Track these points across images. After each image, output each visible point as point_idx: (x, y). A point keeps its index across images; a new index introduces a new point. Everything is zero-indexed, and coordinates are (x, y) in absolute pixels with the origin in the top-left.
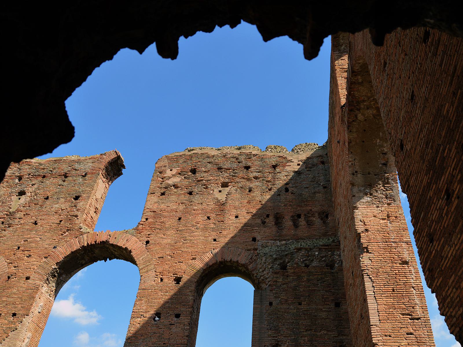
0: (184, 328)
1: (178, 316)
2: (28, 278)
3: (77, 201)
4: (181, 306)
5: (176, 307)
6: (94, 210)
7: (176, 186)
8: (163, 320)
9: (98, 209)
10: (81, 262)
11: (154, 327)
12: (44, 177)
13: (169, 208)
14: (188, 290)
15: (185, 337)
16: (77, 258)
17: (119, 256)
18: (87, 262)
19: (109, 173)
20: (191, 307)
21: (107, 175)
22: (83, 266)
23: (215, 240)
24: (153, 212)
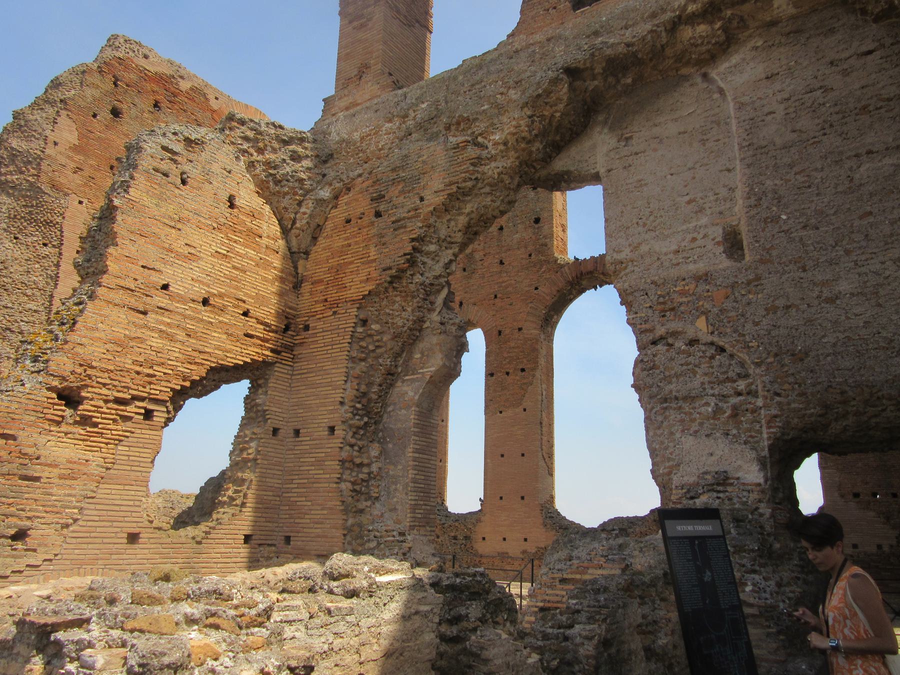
2: (520, 329)
22: (571, 300)
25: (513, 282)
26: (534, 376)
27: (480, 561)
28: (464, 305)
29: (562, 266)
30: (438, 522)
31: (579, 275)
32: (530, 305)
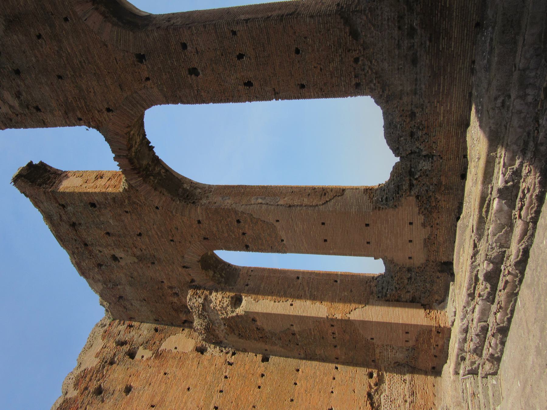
0: (196, 33)
1: (184, 46)
2: (199, 222)
3: (96, 204)
4: (170, 45)
5: (173, 51)
6: (99, 180)
7: (18, 95)
9: (97, 176)
10: (163, 174)
11: (207, 72)
12: (86, 245)
13: (52, 96)
14: (147, 40)
15: (207, 29)
16: (160, 180)
17: (141, 135)
18: (161, 167)
19: (47, 179)
20: (168, 30)
21: (50, 180)
22: (168, 170)
23: (66, 19)
24: (67, 114)
25: (155, 226)
26: (243, 213)
27: (433, 262)
28: (185, 265)
29: (130, 186)
30: (394, 292)
31: (136, 172)
32: (174, 213)
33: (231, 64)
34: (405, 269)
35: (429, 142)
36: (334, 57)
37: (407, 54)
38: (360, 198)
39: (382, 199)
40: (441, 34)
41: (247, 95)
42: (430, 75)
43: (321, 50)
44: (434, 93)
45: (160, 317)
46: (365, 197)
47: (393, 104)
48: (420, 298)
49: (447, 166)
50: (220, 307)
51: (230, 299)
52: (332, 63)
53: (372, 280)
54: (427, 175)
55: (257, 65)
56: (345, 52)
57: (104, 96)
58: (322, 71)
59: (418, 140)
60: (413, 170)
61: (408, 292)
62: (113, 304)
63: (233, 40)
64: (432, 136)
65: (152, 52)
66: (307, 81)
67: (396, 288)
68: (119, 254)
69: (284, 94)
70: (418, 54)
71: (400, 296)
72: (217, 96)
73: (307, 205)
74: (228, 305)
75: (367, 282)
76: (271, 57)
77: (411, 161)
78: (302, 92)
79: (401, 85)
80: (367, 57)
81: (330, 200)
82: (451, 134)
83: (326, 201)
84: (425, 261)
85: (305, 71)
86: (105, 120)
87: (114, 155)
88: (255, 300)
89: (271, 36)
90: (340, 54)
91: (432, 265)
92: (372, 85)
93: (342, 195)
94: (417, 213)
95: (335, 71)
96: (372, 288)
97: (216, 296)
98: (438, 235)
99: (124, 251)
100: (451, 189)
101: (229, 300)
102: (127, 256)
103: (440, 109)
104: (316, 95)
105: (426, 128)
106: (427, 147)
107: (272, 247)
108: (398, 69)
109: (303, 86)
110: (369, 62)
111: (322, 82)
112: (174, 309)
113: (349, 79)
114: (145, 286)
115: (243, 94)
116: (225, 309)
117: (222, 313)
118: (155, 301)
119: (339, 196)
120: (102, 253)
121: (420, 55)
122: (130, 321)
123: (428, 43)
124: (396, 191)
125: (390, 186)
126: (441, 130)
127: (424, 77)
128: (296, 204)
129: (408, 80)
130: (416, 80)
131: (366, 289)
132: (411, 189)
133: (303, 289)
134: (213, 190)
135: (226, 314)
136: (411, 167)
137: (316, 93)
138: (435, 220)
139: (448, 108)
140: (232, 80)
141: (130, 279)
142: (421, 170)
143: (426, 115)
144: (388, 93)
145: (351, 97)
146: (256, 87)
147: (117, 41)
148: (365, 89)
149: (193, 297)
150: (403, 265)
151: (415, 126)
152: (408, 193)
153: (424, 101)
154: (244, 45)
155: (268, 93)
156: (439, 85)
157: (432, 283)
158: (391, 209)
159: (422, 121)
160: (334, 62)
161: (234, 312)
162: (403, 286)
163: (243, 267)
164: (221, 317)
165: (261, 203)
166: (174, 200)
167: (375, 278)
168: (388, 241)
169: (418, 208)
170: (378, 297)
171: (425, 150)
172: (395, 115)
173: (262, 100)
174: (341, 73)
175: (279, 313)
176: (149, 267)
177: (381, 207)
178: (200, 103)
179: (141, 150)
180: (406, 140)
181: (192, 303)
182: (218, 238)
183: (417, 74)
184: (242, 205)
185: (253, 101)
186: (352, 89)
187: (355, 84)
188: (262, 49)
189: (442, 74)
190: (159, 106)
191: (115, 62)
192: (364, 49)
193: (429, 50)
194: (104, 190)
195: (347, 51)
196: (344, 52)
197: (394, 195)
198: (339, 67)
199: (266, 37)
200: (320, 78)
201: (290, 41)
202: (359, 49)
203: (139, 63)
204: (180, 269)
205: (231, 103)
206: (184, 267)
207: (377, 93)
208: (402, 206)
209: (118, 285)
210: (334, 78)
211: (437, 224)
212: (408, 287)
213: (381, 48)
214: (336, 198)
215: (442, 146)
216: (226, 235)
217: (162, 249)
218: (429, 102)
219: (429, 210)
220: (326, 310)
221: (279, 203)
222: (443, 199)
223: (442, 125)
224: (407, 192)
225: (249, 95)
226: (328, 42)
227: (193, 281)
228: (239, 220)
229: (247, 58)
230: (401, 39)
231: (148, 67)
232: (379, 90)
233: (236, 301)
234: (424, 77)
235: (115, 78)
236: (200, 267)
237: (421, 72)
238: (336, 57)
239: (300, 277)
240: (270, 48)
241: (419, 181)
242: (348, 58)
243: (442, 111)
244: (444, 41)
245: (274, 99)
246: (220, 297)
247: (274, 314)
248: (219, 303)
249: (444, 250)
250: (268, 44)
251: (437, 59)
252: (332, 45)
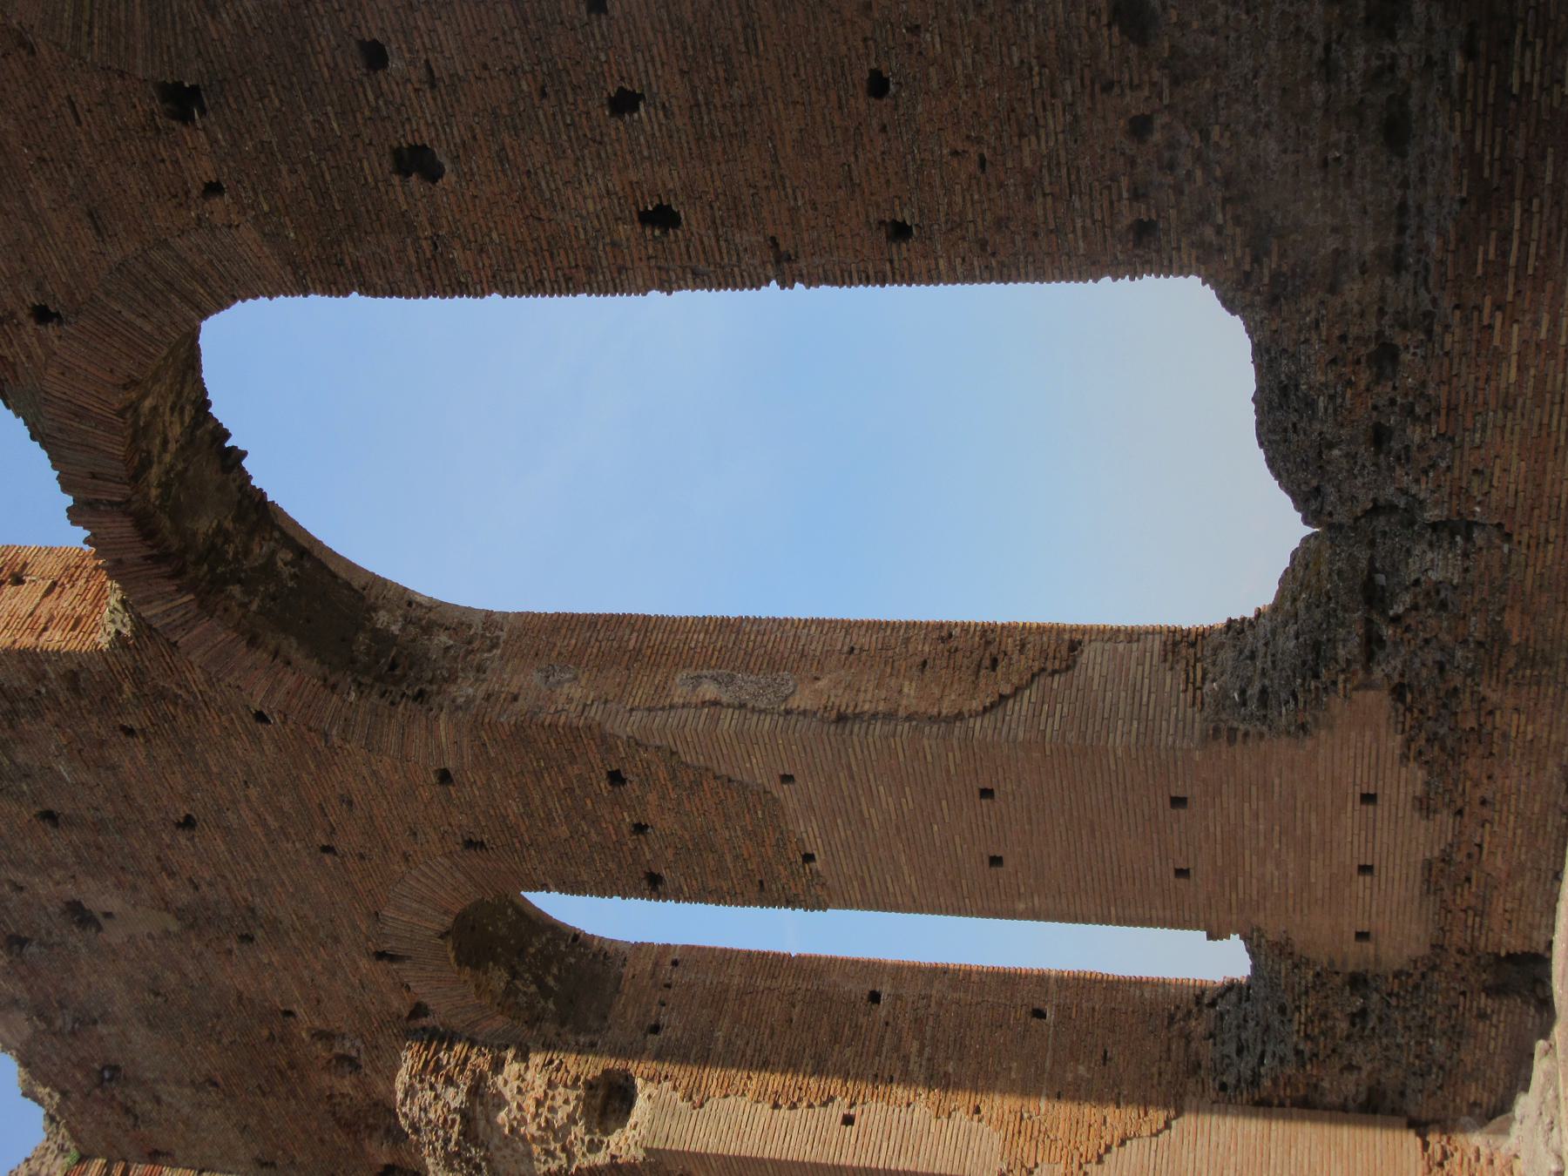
1: (375, 55)
2: (445, 777)
4: (312, 48)
5: (326, 74)
8: (423, 128)
10: (286, 571)
11: (474, 165)
14: (211, 27)
16: (274, 599)
18: (276, 540)
25: (253, 792)
26: (635, 743)
27: (1460, 951)
28: (386, 947)
29: (141, 626)
31: (165, 569)
32: (337, 741)
33: (580, 133)
34: (1338, 980)
35: (1456, 473)
36: (1040, 113)
37: (1362, 101)
38: (1146, 681)
39: (1243, 692)
40: (1520, 27)
41: (653, 262)
42: (1464, 194)
43: (985, 82)
44: (1480, 271)
45: (280, 1153)
46: (1168, 681)
47: (1298, 311)
48: (1402, 1094)
49: (1531, 570)
50: (539, 1127)
51: (581, 1092)
52: (1033, 138)
53: (1195, 1010)
54: (1443, 605)
55: (698, 140)
56: (1092, 96)
57: (23, 260)
58: (988, 165)
59: (1408, 460)
60: (1381, 579)
61: (1350, 1067)
62: (76, 1096)
63: (593, 35)
64: (1467, 446)
65: (230, 75)
66: (920, 210)
67: (1298, 1053)
68: (100, 897)
69: (817, 260)
70: (1413, 103)
71: (1316, 1086)
72: (519, 266)
73: (916, 713)
74: (572, 1120)
75: (1172, 1018)
76: (763, 108)
77: (1372, 544)
78: (899, 253)
79: (1335, 230)
80: (1186, 113)
81: (1017, 691)
82: (1553, 439)
83: (1001, 697)
84: (1427, 951)
85: (911, 168)
86: (29, 357)
87: (68, 500)
88: (691, 1098)
89: (760, 19)
90: (1070, 98)
91: (1458, 966)
92: (1209, 232)
93: (1068, 668)
94: (1397, 757)
95: (1045, 171)
96: (1193, 1045)
97: (520, 1077)
98: (1485, 846)
99: (119, 885)
100: (1548, 662)
101: (577, 1098)
102: (134, 906)
103: (1506, 336)
104: (959, 270)
105: (1443, 412)
106: (1446, 490)
107: (761, 882)
108: (1325, 164)
109: (900, 231)
110: (1197, 138)
111: (988, 216)
112: (338, 1121)
113: (1106, 204)
114: (213, 1027)
115: (636, 256)
116: (561, 1134)
117: (550, 1154)
118: (259, 1086)
119: (1054, 672)
120: (25, 894)
121: (1424, 108)
122: (154, 1163)
123: (1458, 62)
124: (1304, 663)
125: (1280, 640)
126: (1509, 425)
127: (1439, 200)
128: (866, 707)
129: (1365, 212)
130: (1403, 208)
131: (1169, 1049)
132: (1370, 657)
133: (897, 1049)
134: (504, 635)
135: (563, 1156)
136: (1372, 570)
137: (959, 260)
138: (1476, 785)
139: (1543, 335)
140: (585, 198)
141: (150, 999)
142: (1417, 582)
143: (1446, 361)
144: (1279, 266)
145: (1115, 279)
146: (694, 229)
147: (77, 27)
148: (1179, 249)
149: (422, 1081)
150: (1332, 962)
151: (1393, 402)
152: (1361, 674)
153: (1434, 301)
154: (639, 56)
155: (746, 257)
156: (1505, 237)
157: (1456, 1035)
158: (1284, 740)
159: (1424, 384)
160: (1042, 132)
161: (599, 1149)
162: (1330, 1046)
163: (638, 947)
164: (544, 1168)
165: (716, 703)
166: (334, 687)
167: (1206, 1001)
168: (1270, 866)
169: (1399, 738)
170: (1223, 1087)
171: (1436, 504)
172: (1309, 357)
173: (719, 287)
174: (1073, 177)
175: (792, 1156)
176: (230, 952)
177: (1237, 729)
178: (444, 295)
179: (190, 473)
180: (1352, 457)
181: (416, 1109)
182: (527, 841)
183: (1405, 184)
184: (632, 710)
185: (680, 288)
186: (1119, 247)
187: (1130, 227)
188: (721, 74)
189: (1517, 193)
190: (263, 300)
191: (71, 121)
192: (1175, 82)
193: (1463, 92)
194: (27, 641)
195: (1097, 87)
196: (1088, 90)
197: (1299, 681)
198: (1062, 153)
199: (737, 23)
200: (976, 197)
201: (846, 41)
202: (1155, 80)
203: (174, 123)
204: (364, 964)
205: (582, 297)
206: (380, 955)
207: (1231, 264)
208: (1330, 727)
209: (95, 1022)
210: (1040, 200)
211: (1483, 802)
212: (1350, 1049)
213: (1250, 76)
214: (1043, 680)
215: (1512, 487)
216: (564, 831)
217: (283, 884)
218: (1457, 307)
219: (1449, 743)
220: (998, 1146)
221: (794, 703)
222: (1510, 702)
223: (1515, 401)
224: (1355, 673)
225: (662, 263)
226: (1014, 48)
227: (419, 1010)
228: (618, 771)
229: (652, 110)
230: (1340, 36)
231: (213, 141)
232: (1239, 254)
233: (608, 1098)
234: (1439, 200)
235: (71, 182)
236: (452, 955)
237: (1423, 180)
238: (1049, 114)
239: (886, 990)
240: (756, 70)
241: (1408, 629)
242: (1104, 118)
243: (1515, 342)
244: (1528, 54)
245: (773, 283)
246: (538, 1082)
247: (773, 1162)
248: (532, 1109)
249: (1508, 906)
250: (749, 53)
251: (1499, 130)
252: (1034, 62)
